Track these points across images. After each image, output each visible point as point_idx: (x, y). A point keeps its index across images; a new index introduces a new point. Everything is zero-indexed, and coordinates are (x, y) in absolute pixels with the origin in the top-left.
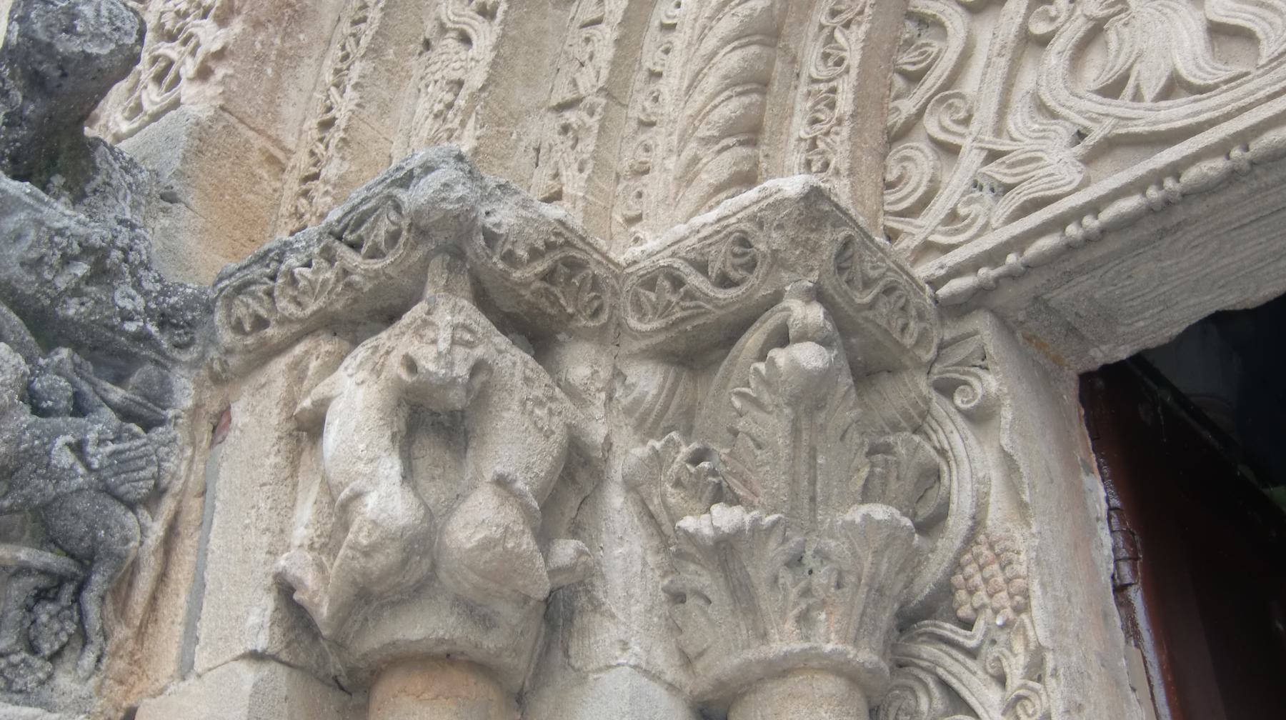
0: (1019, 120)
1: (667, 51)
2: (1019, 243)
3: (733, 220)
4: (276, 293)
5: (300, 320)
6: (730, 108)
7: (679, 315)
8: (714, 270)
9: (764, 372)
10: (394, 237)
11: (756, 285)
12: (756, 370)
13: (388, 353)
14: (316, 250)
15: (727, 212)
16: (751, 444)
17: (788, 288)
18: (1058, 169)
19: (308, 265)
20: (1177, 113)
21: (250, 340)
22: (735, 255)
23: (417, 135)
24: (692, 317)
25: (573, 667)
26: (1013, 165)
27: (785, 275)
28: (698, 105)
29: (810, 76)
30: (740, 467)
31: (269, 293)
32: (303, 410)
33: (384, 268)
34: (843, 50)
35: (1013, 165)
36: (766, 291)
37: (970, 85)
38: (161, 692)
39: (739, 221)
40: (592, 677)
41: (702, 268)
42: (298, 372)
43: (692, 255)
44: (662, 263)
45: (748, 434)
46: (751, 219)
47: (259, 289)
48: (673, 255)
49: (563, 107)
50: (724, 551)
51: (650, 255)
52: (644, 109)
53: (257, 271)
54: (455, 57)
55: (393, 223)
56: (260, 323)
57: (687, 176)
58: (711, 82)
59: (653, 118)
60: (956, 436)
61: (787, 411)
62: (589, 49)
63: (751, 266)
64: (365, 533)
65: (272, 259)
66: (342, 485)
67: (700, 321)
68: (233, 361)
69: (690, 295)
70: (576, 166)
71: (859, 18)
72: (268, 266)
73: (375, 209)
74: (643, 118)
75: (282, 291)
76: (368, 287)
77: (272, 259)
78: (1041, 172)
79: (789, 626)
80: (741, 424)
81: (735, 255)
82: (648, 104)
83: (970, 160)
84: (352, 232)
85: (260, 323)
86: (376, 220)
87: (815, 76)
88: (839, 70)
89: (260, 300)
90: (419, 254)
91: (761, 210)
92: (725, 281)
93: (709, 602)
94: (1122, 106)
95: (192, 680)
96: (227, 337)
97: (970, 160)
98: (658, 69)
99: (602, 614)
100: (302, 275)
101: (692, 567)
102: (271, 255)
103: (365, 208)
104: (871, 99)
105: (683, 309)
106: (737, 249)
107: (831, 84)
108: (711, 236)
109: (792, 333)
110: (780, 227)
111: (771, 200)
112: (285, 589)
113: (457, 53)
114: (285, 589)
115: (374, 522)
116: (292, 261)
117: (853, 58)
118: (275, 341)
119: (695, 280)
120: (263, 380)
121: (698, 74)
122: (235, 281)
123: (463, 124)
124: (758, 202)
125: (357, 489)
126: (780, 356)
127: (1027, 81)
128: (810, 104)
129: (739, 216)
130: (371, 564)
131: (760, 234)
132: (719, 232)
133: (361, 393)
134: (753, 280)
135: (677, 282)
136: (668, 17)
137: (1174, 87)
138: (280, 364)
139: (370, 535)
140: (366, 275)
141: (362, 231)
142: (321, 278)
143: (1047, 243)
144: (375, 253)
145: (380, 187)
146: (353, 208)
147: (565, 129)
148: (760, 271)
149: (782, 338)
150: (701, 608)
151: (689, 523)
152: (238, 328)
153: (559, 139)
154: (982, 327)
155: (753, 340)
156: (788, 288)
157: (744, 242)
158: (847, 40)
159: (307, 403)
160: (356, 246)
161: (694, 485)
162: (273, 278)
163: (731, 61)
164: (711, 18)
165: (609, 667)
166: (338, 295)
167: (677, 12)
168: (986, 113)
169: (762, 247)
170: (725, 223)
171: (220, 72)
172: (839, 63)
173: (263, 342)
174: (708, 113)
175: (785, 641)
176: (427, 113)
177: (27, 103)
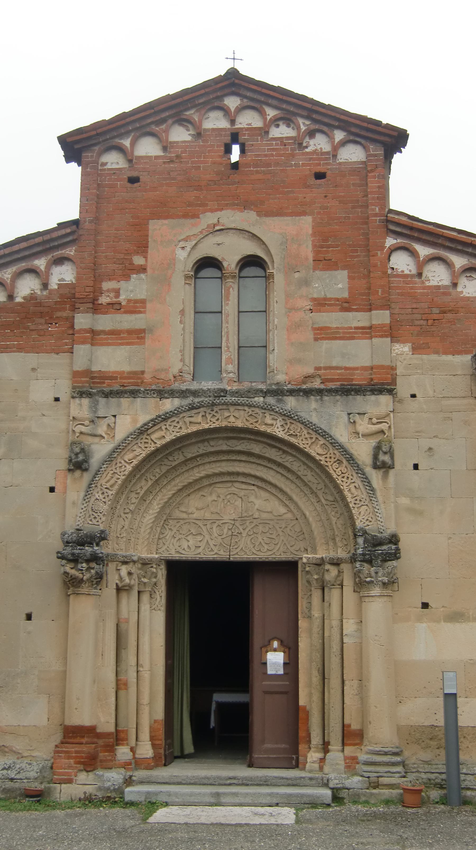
0: (171, 545)
2: (168, 557)
6: (148, 537)
18: (173, 552)
20: (183, 552)
37: (167, 537)
42: (117, 565)
50: (145, 583)
57: (143, 543)
58: (147, 533)
60: (159, 570)
83: (166, 547)
94: (179, 548)
97: (166, 547)
104: (159, 536)
112: (117, 584)
114: (117, 584)
117: (158, 532)
126: (152, 569)
127: (173, 540)
137: (184, 549)
138: (115, 563)
143: (171, 558)
149: (152, 567)
151: (142, 579)
154: (163, 562)
159: (118, 568)
163: (149, 531)
168: (168, 542)
171: (104, 523)
175: (147, 589)
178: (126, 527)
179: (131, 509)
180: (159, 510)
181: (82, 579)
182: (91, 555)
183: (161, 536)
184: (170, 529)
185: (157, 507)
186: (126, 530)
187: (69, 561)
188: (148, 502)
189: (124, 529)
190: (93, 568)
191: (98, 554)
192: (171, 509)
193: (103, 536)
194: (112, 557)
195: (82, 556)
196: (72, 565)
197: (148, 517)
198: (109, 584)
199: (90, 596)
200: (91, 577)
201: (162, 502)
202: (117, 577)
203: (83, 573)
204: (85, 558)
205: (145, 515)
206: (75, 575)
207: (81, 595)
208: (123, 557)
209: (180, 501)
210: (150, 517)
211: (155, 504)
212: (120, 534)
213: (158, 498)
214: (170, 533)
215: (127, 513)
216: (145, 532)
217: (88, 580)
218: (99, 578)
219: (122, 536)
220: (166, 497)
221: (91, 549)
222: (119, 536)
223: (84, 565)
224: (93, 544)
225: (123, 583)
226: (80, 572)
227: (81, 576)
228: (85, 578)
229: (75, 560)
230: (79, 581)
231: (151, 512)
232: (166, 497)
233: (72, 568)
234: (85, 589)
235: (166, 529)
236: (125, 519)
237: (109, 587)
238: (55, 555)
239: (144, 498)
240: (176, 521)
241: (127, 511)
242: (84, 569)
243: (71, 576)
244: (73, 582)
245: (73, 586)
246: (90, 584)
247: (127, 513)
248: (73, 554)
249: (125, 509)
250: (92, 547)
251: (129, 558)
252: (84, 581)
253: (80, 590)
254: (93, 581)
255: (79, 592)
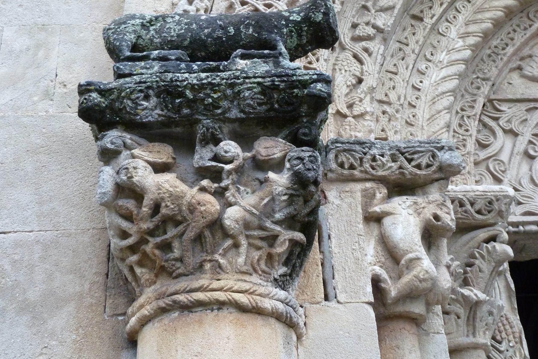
1: (417, 98)
2: (524, 224)
3: (489, 194)
4: (365, 160)
5: (372, 175)
7: (460, 216)
8: (477, 207)
9: (490, 249)
10: (428, 166)
11: (489, 218)
12: (486, 247)
13: (423, 208)
14: (388, 153)
15: (487, 190)
16: (478, 270)
17: (500, 223)
19: (382, 156)
21: (346, 172)
22: (486, 206)
23: (339, 90)
24: (464, 219)
25: (423, 329)
26: (523, 196)
27: (500, 219)
28: (437, 129)
29: (454, 129)
30: (472, 276)
31: (361, 159)
32: (376, 212)
33: (420, 175)
34: (468, 126)
35: (523, 196)
36: (492, 221)
38: (318, 303)
39: (492, 195)
40: (431, 335)
41: (472, 204)
43: (471, 199)
44: (459, 196)
45: (479, 267)
46: (495, 196)
47: (358, 156)
48: (464, 195)
49: (381, 102)
51: (455, 191)
52: (409, 118)
53: (358, 148)
54: (355, 65)
55: (430, 161)
56: (352, 167)
59: (413, 123)
61: (493, 264)
62: (392, 84)
63: (489, 212)
64: (422, 274)
65: (367, 147)
66: (406, 252)
67: (464, 221)
68: (330, 175)
69: (466, 212)
70: (393, 131)
71: (474, 117)
72: (364, 148)
73: (422, 152)
74: (408, 120)
75: (368, 162)
76: (409, 177)
77: (367, 147)
78: (534, 204)
79: (481, 333)
80: (477, 262)
81: (486, 206)
82: (411, 116)
84: (409, 155)
85: (352, 167)
86: (422, 156)
87: (456, 130)
88: (467, 133)
89: (355, 158)
90: (436, 176)
91: (500, 195)
92: (479, 212)
93: (459, 318)
95: (333, 304)
96: (334, 166)
98: (414, 104)
99: (433, 313)
100: (380, 159)
101: (458, 305)
102: (367, 145)
103: (419, 149)
105: (462, 215)
106: (488, 204)
107: (465, 137)
108: (479, 195)
109: (497, 239)
110: (506, 204)
111: (505, 193)
112: (376, 282)
113: (355, 63)
115: (427, 271)
116: (374, 151)
118: (357, 177)
119: (469, 207)
120: (347, 189)
121: (433, 116)
122: (346, 147)
123: (365, 97)
124: (498, 192)
125: (419, 256)
128: (455, 140)
129: (492, 193)
130: (420, 285)
131: (496, 203)
132: (483, 195)
133: (411, 218)
134: (489, 216)
135: (462, 205)
136: (417, 85)
138: (358, 187)
139: (424, 275)
140: (410, 174)
141: (416, 156)
142: (389, 165)
144: (418, 167)
145: (427, 145)
146: (413, 147)
147: (384, 113)
148: (492, 214)
150: (455, 319)
152: (342, 165)
153: (381, 115)
155: (483, 234)
156: (500, 223)
157: (490, 203)
158: (470, 123)
159: (377, 209)
160: (410, 161)
161: (455, 276)
162: (365, 154)
164: (437, 96)
165: (438, 333)
166: (396, 174)
167: (421, 84)
169: (497, 207)
170: (486, 194)
172: (467, 131)
173: (352, 175)
174: (441, 134)
176: (344, 83)
177: (308, 45)
178: (369, 81)
179: (380, 23)
180: (468, 53)
181: (216, 225)
182: (265, 90)
183: (483, 154)
184: (512, 133)
185: (460, 43)
186: (372, 90)
187: (148, 132)
188: (428, 21)
189: (364, 86)
190: (277, 166)
191: (304, 84)
192: (501, 64)
193: (319, 17)
194: (342, 158)
195: (215, 105)
196: (163, 153)
197: (435, 75)
198: (339, 282)
199: (259, 321)
200: (268, 211)
201: (473, 28)
202: (371, 250)
203: (219, 194)
204: (234, 113)
205: (450, 17)
206: (177, 198)
207: (209, 316)
208: (394, 159)
209: (519, 49)
210: (444, 73)
211: (453, 33)
212: (350, 106)
213: (461, 18)
214: (508, 142)
215: (369, 38)
216: (431, 119)
217: (247, 226)
218: (297, 237)
219: (357, 110)
220: (488, 15)
221: (263, 67)
222: (345, 111)
223: (230, 147)
224: (273, 47)
225: (406, 278)
226: (205, 183)
227: (212, 204)
228: (233, 216)
229: (179, 126)
230: (199, 239)
231: (442, 56)
232: (488, 15)
233: (159, 168)
234: (236, 277)
235: (494, 133)
236: (364, 56)
237: (341, 297)
238: (75, 101)
239: (416, 11)
240: (524, 107)
241: (371, 31)
242: (228, 167)
243: (156, 208)
244: (166, 247)
245: (163, 271)
246: (256, 254)
247: (369, 38)
248: (169, 92)
249: (355, 26)
250: (276, 58)
251: (424, 161)
252: (226, 235)
253: (204, 281)
254: (272, 240)
255: (200, 296)
